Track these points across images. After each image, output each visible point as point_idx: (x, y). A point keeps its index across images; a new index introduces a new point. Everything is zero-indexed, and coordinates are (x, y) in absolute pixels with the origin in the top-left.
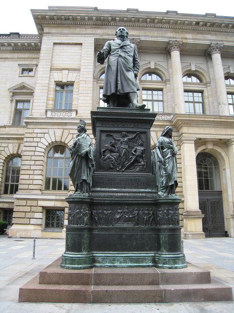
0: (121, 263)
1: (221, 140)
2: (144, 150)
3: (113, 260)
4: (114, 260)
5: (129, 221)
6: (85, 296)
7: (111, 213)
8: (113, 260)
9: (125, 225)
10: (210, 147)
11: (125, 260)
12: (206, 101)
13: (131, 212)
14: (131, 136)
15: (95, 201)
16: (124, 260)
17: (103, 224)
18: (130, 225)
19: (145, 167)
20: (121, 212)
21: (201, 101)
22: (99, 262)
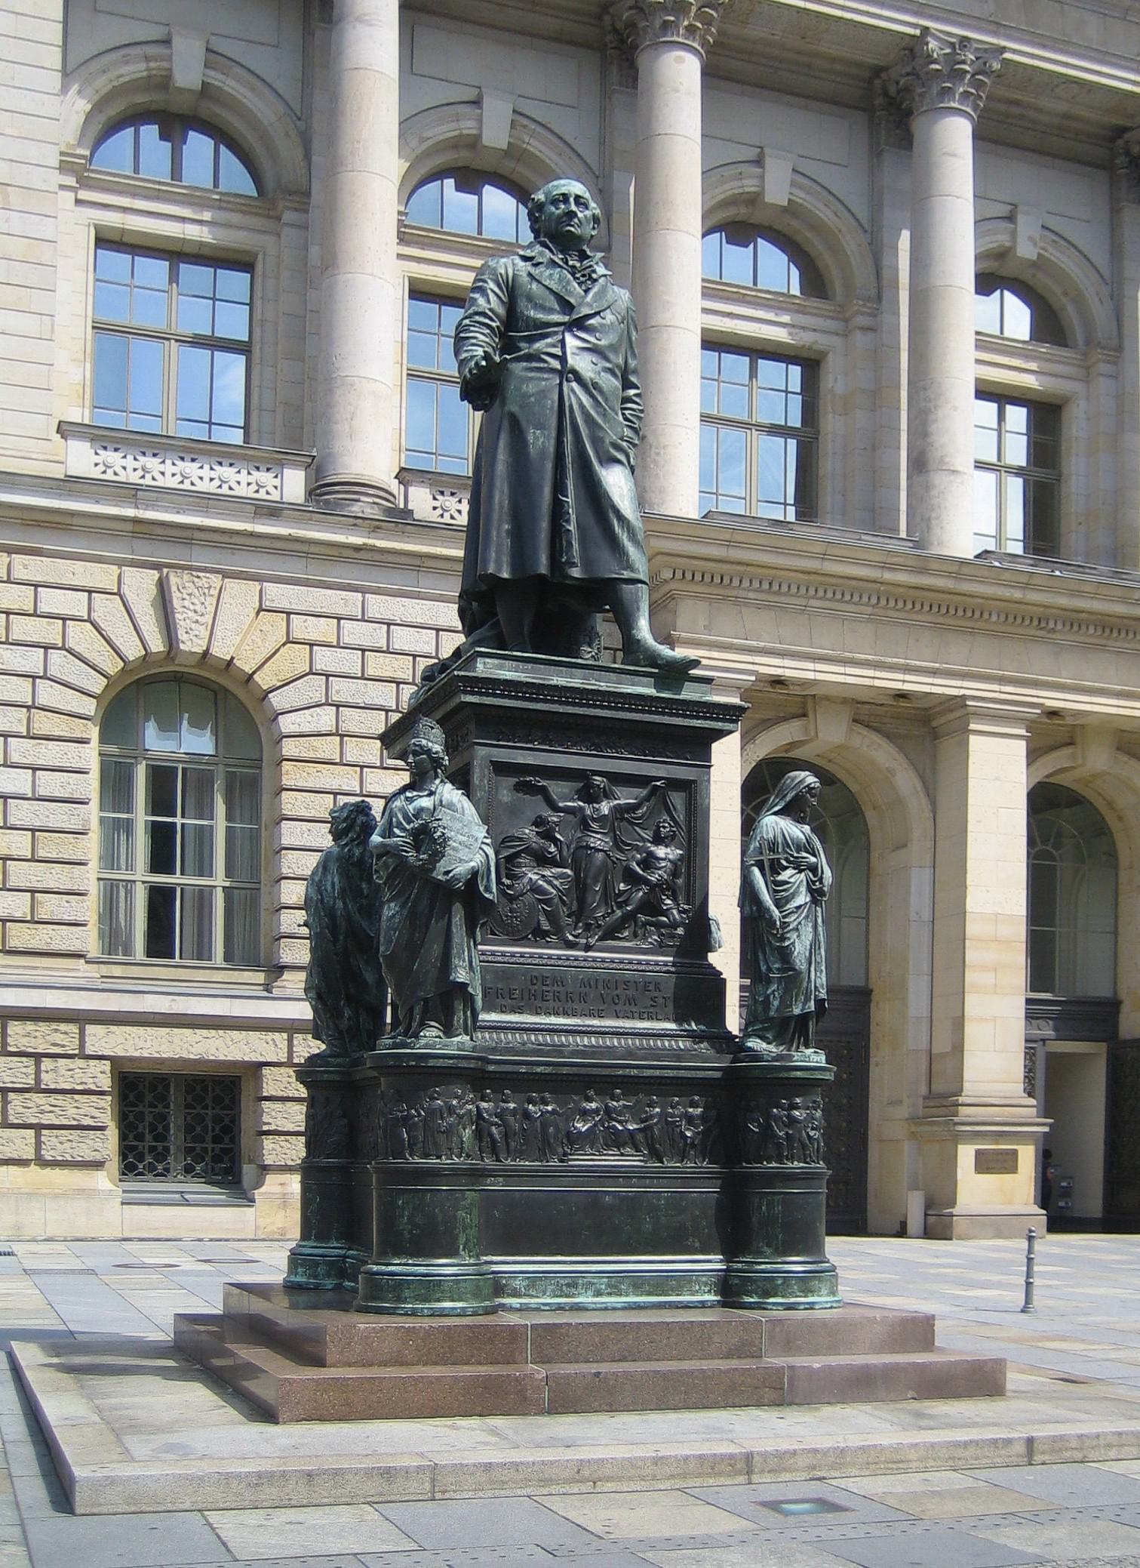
0: (598, 1294)
1: (902, 695)
2: (681, 858)
3: (568, 1285)
4: (573, 1285)
5: (624, 1145)
6: (521, 1393)
7: (554, 1111)
8: (568, 1285)
9: (611, 1159)
10: (831, 734)
11: (616, 1283)
12: (831, 424)
13: (635, 1112)
14: (626, 797)
15: (491, 1068)
16: (608, 1285)
17: (521, 1154)
18: (631, 1160)
19: (680, 931)
20: (596, 1111)
21: (795, 421)
22: (516, 1294)
